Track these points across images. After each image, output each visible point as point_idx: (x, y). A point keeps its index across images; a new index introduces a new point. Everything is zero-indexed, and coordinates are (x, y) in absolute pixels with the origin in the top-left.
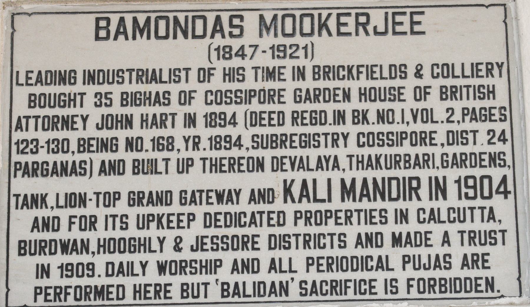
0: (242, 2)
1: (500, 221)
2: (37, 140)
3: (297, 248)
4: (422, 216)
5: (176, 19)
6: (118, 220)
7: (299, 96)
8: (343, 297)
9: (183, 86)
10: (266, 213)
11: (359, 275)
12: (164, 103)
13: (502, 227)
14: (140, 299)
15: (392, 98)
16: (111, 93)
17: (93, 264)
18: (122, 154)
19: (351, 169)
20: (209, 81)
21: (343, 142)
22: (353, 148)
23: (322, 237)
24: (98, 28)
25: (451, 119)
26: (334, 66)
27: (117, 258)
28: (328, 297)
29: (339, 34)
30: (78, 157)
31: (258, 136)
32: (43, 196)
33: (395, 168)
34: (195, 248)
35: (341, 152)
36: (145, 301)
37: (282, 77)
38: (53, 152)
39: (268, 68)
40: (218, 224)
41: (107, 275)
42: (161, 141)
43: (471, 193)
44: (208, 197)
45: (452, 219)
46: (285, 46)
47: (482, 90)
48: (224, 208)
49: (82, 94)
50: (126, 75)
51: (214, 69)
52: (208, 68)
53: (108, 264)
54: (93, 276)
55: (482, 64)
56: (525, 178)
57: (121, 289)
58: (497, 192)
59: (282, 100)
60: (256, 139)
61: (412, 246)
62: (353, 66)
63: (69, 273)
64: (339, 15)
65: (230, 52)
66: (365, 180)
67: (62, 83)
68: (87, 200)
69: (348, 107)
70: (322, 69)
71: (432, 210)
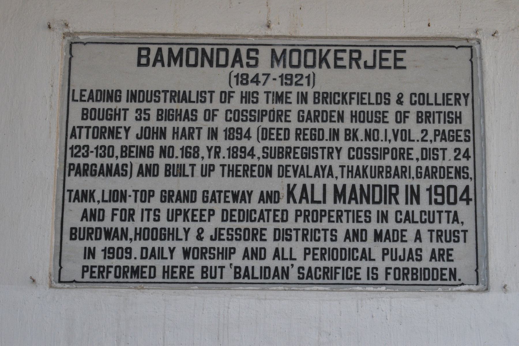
0: (257, 39)
1: (462, 223)
3: (297, 240)
4: (399, 217)
5: (203, 50)
6: (152, 213)
7: (302, 116)
9: (208, 105)
10: (272, 211)
11: (346, 264)
12: (192, 119)
13: (464, 228)
14: (168, 278)
15: (378, 120)
16: (149, 110)
17: (130, 249)
18: (156, 159)
19: (342, 177)
20: (229, 102)
21: (337, 154)
22: (344, 160)
23: (317, 232)
24: (140, 56)
25: (425, 139)
26: (331, 93)
27: (150, 244)
28: (321, 281)
29: (336, 66)
31: (267, 148)
32: (92, 192)
33: (379, 177)
34: (214, 238)
35: (335, 163)
36: (171, 279)
37: (288, 100)
38: (101, 156)
39: (277, 93)
40: (233, 218)
41: (142, 258)
42: (189, 150)
43: (440, 199)
44: (226, 197)
45: (423, 220)
46: (291, 75)
47: (451, 115)
48: (238, 206)
49: (126, 110)
50: (162, 95)
51: (234, 92)
52: (229, 92)
53: (142, 248)
54: (130, 258)
55: (451, 94)
56: (483, 188)
57: (152, 269)
58: (461, 199)
59: (288, 119)
60: (266, 150)
61: (390, 241)
62: (346, 93)
63: (111, 256)
64: (336, 51)
66: (354, 186)
69: (341, 127)
70: (321, 95)
71: (408, 212)
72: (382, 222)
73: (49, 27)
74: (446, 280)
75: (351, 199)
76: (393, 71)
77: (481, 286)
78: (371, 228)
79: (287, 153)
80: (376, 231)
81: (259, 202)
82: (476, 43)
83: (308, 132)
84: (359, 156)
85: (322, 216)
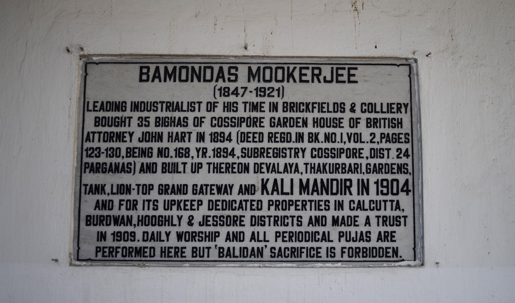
0: (237, 58)
1: (403, 210)
2: (99, 148)
3: (269, 225)
4: (352, 205)
5: (193, 68)
6: (151, 203)
7: (273, 122)
8: (299, 259)
9: (197, 114)
10: (250, 201)
11: (310, 244)
12: (183, 125)
13: (404, 214)
14: (165, 257)
15: (335, 125)
16: (149, 117)
17: (134, 233)
18: (155, 159)
19: (306, 173)
20: (214, 111)
21: (302, 154)
22: (308, 158)
23: (286, 218)
24: (141, 74)
25: (373, 140)
27: (150, 229)
28: (289, 259)
29: (301, 81)
32: (103, 186)
34: (202, 224)
35: (300, 161)
36: (168, 258)
37: (262, 109)
38: (110, 157)
39: (253, 103)
40: (218, 207)
41: (144, 240)
42: (181, 151)
43: (385, 190)
44: (212, 190)
45: (372, 208)
46: (265, 88)
47: (394, 122)
48: (221, 197)
49: (130, 118)
50: (159, 106)
51: (218, 103)
52: (214, 102)
53: (144, 233)
54: (134, 240)
55: (394, 104)
56: (420, 181)
57: (152, 250)
58: (402, 190)
59: (262, 125)
60: (244, 151)
61: (345, 226)
62: (309, 103)
63: (119, 238)
64: (301, 69)
65: (228, 92)
66: (315, 180)
67: (117, 111)
68: (132, 189)
69: (305, 131)
70: (289, 104)
71: (359, 201)
73: (68, 51)
74: (390, 257)
75: (313, 191)
76: (347, 85)
77: (418, 262)
78: (330, 214)
80: (333, 217)
81: (239, 194)
82: (414, 62)
83: (278, 135)
84: (320, 155)
85: (290, 205)
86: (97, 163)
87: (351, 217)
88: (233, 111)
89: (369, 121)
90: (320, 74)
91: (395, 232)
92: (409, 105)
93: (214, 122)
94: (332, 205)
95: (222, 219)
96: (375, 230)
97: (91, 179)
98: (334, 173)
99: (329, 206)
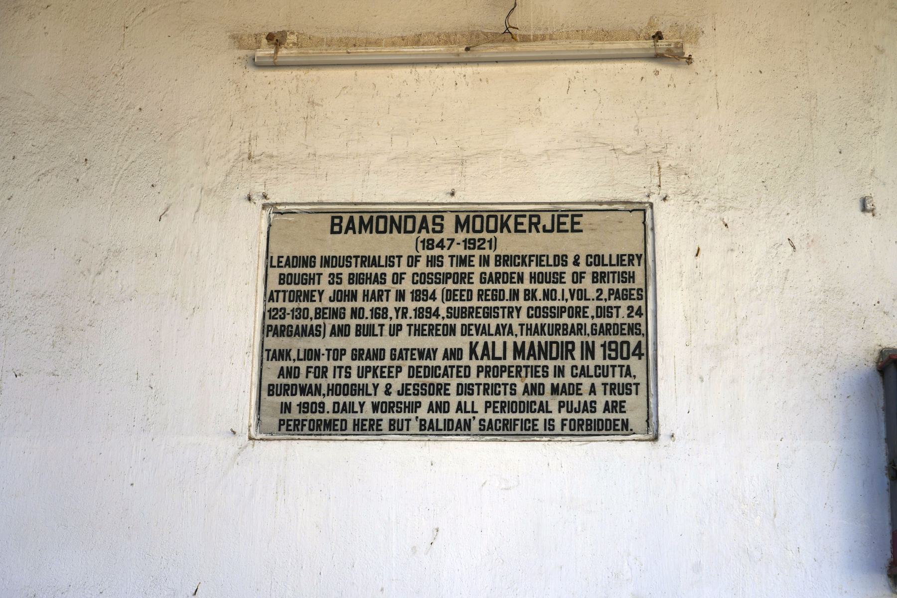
1: (635, 376)
2: (285, 309)
3: (478, 394)
4: (575, 371)
5: (392, 217)
6: (343, 370)
7: (484, 278)
8: (513, 432)
9: (396, 269)
10: (456, 367)
11: (525, 416)
12: (381, 282)
13: (636, 381)
15: (555, 280)
16: (341, 274)
17: (324, 403)
19: (522, 335)
20: (416, 266)
22: (524, 318)
23: (497, 386)
24: (333, 225)
25: (600, 297)
26: (511, 256)
27: (342, 399)
28: (501, 432)
29: (517, 231)
30: (315, 322)
31: (451, 308)
33: (556, 335)
34: (401, 393)
35: (515, 322)
37: (471, 263)
38: (297, 318)
39: (461, 256)
40: (419, 374)
41: (334, 412)
42: (378, 311)
43: (613, 354)
44: (412, 354)
45: (598, 374)
46: (474, 240)
47: (624, 275)
48: (424, 363)
49: (320, 275)
50: (353, 261)
51: (420, 256)
52: (416, 256)
53: (335, 403)
54: (323, 412)
55: (625, 255)
57: (344, 422)
58: (634, 354)
62: (526, 256)
63: (306, 410)
64: (516, 217)
65: (432, 244)
66: (532, 343)
68: (321, 355)
70: (502, 257)
71: (583, 367)
72: (559, 377)
78: (548, 382)
79: (469, 312)
80: (552, 384)
81: (443, 359)
83: (489, 293)
84: (538, 315)
85: (502, 372)
86: (282, 326)
87: (573, 384)
88: (438, 266)
89: (595, 275)
90: (539, 222)
91: (625, 402)
92: (643, 256)
93: (416, 278)
94: (551, 371)
95: (424, 387)
96: (601, 399)
97: (275, 343)
98: (554, 335)
99: (547, 372)
